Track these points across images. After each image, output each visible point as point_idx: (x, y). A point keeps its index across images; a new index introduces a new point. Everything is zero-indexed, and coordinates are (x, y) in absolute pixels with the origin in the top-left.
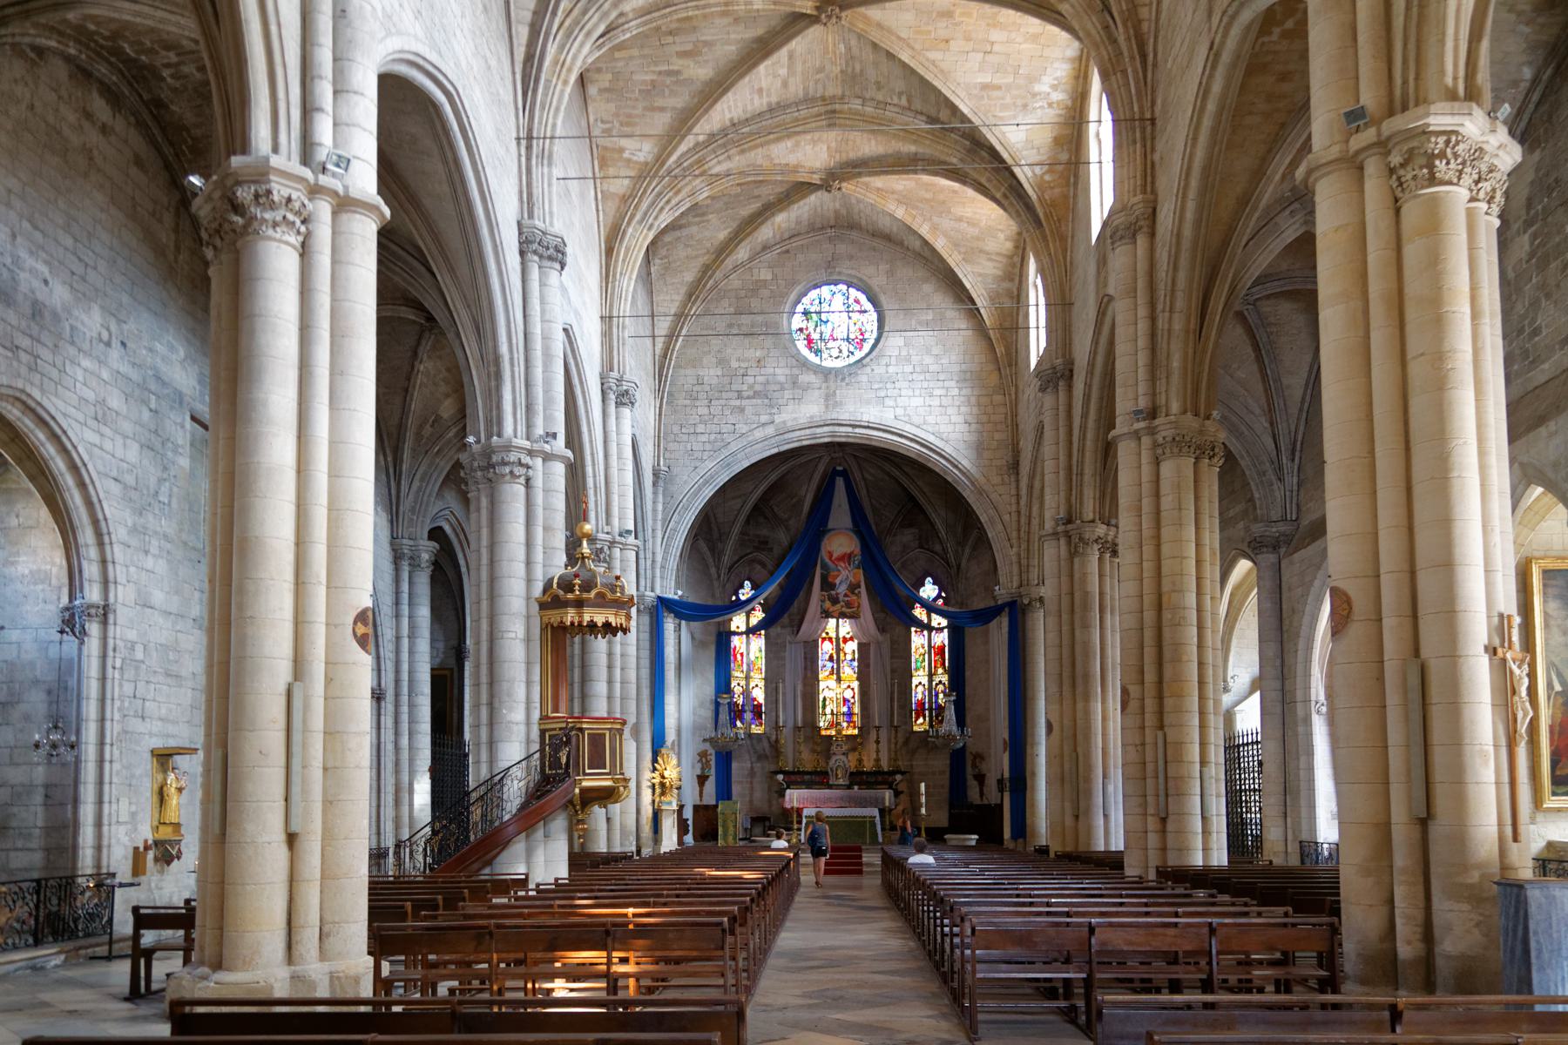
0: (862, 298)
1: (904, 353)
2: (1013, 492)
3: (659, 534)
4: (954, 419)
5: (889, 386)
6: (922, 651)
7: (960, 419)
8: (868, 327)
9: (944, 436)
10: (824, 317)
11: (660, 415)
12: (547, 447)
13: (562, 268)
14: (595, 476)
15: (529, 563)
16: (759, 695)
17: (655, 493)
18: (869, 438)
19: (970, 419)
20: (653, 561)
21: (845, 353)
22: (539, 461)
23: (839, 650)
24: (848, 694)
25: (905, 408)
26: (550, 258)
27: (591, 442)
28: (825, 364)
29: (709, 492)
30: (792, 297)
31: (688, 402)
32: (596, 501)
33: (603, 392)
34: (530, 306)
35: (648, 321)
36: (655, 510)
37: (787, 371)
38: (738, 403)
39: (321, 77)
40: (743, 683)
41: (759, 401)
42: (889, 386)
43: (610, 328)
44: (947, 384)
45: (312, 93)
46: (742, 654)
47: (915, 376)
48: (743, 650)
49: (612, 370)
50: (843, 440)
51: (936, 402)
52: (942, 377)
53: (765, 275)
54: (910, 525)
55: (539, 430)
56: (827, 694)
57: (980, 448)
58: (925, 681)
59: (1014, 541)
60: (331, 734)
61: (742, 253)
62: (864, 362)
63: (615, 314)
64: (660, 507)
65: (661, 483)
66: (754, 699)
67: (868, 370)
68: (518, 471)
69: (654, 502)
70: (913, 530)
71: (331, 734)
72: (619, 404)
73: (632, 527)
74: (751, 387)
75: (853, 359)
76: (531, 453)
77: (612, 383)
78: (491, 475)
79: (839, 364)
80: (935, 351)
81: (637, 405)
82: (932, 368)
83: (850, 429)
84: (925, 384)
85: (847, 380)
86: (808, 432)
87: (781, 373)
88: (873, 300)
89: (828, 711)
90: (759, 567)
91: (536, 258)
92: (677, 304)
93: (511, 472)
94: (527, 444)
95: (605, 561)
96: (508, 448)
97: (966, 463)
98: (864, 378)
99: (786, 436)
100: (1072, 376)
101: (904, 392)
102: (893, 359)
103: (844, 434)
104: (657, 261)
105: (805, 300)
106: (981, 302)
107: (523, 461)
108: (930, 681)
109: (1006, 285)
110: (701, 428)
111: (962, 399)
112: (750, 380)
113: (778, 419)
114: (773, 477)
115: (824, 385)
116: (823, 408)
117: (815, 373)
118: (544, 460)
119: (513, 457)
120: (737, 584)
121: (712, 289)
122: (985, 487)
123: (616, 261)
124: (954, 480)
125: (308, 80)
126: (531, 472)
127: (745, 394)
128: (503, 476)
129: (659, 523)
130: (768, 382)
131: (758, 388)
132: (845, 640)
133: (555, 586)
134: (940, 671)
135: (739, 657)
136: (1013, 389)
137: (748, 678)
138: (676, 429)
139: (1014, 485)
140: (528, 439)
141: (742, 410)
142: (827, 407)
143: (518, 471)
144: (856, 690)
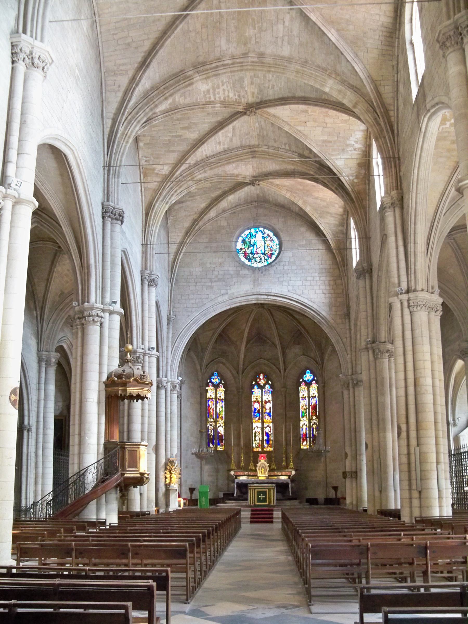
0: (271, 234)
1: (292, 260)
2: (348, 327)
3: (170, 349)
4: (317, 292)
5: (285, 275)
6: (305, 407)
7: (321, 292)
8: (274, 247)
9: (313, 300)
10: (252, 243)
11: (171, 290)
12: (111, 308)
13: (122, 224)
14: (136, 321)
15: (100, 364)
16: (221, 430)
17: (168, 329)
18: (275, 301)
19: (325, 291)
20: (167, 363)
21: (263, 260)
22: (107, 314)
23: (263, 407)
24: (267, 430)
25: (293, 286)
26: (116, 219)
27: (135, 304)
28: (253, 265)
29: (195, 328)
30: (237, 233)
31: (185, 284)
32: (137, 333)
33: (142, 280)
34: (105, 241)
35: (166, 246)
36: (168, 337)
37: (235, 269)
38: (210, 284)
39: (12, 148)
40: (213, 424)
41: (220, 283)
42: (285, 275)
43: (146, 249)
44: (313, 275)
45: (8, 155)
46: (213, 409)
47: (297, 271)
48: (213, 407)
49: (146, 269)
50: (262, 302)
51: (308, 283)
52: (311, 271)
53: (224, 223)
54: (299, 344)
55: (108, 300)
56: (257, 430)
57: (331, 306)
58: (307, 423)
59: (349, 352)
61: (212, 213)
62: (273, 264)
63: (149, 243)
64: (171, 335)
65: (171, 323)
66: (219, 433)
67: (274, 268)
68: (96, 319)
69: (168, 333)
70: (300, 346)
72: (149, 286)
73: (154, 346)
74: (216, 276)
75: (266, 263)
76: (103, 311)
77: (146, 275)
78: (83, 321)
79: (260, 265)
80: (307, 259)
81: (158, 286)
82: (305, 267)
83: (266, 297)
84: (303, 275)
85: (264, 273)
86: (245, 298)
87: (232, 270)
88: (276, 234)
89: (257, 438)
90: (221, 365)
91: (110, 219)
92: (180, 237)
93: (93, 320)
94: (101, 306)
95: (141, 363)
96: (92, 308)
97: (324, 313)
98: (272, 272)
99: (234, 300)
100: (372, 272)
101: (292, 279)
102: (287, 263)
103: (263, 299)
104: (171, 218)
105: (243, 235)
106: (329, 236)
107: (99, 314)
108: (310, 423)
109: (341, 228)
110: (191, 297)
111: (321, 282)
112: (216, 273)
113: (230, 292)
114: (229, 320)
115: (253, 275)
116: (252, 286)
117: (248, 269)
118: (110, 314)
119: (94, 313)
120: (210, 373)
121: (197, 230)
122: (334, 325)
123: (150, 219)
124: (318, 322)
125: (7, 150)
126: (103, 320)
127: (214, 280)
128: (89, 321)
129: (170, 344)
130: (225, 274)
131: (220, 277)
132: (266, 402)
133: (113, 376)
134: (314, 417)
135: (211, 411)
136: (346, 277)
137: (216, 422)
138: (179, 297)
139: (347, 324)
140: (102, 304)
141: (212, 287)
142: (254, 285)
143: (96, 319)
144: (272, 428)
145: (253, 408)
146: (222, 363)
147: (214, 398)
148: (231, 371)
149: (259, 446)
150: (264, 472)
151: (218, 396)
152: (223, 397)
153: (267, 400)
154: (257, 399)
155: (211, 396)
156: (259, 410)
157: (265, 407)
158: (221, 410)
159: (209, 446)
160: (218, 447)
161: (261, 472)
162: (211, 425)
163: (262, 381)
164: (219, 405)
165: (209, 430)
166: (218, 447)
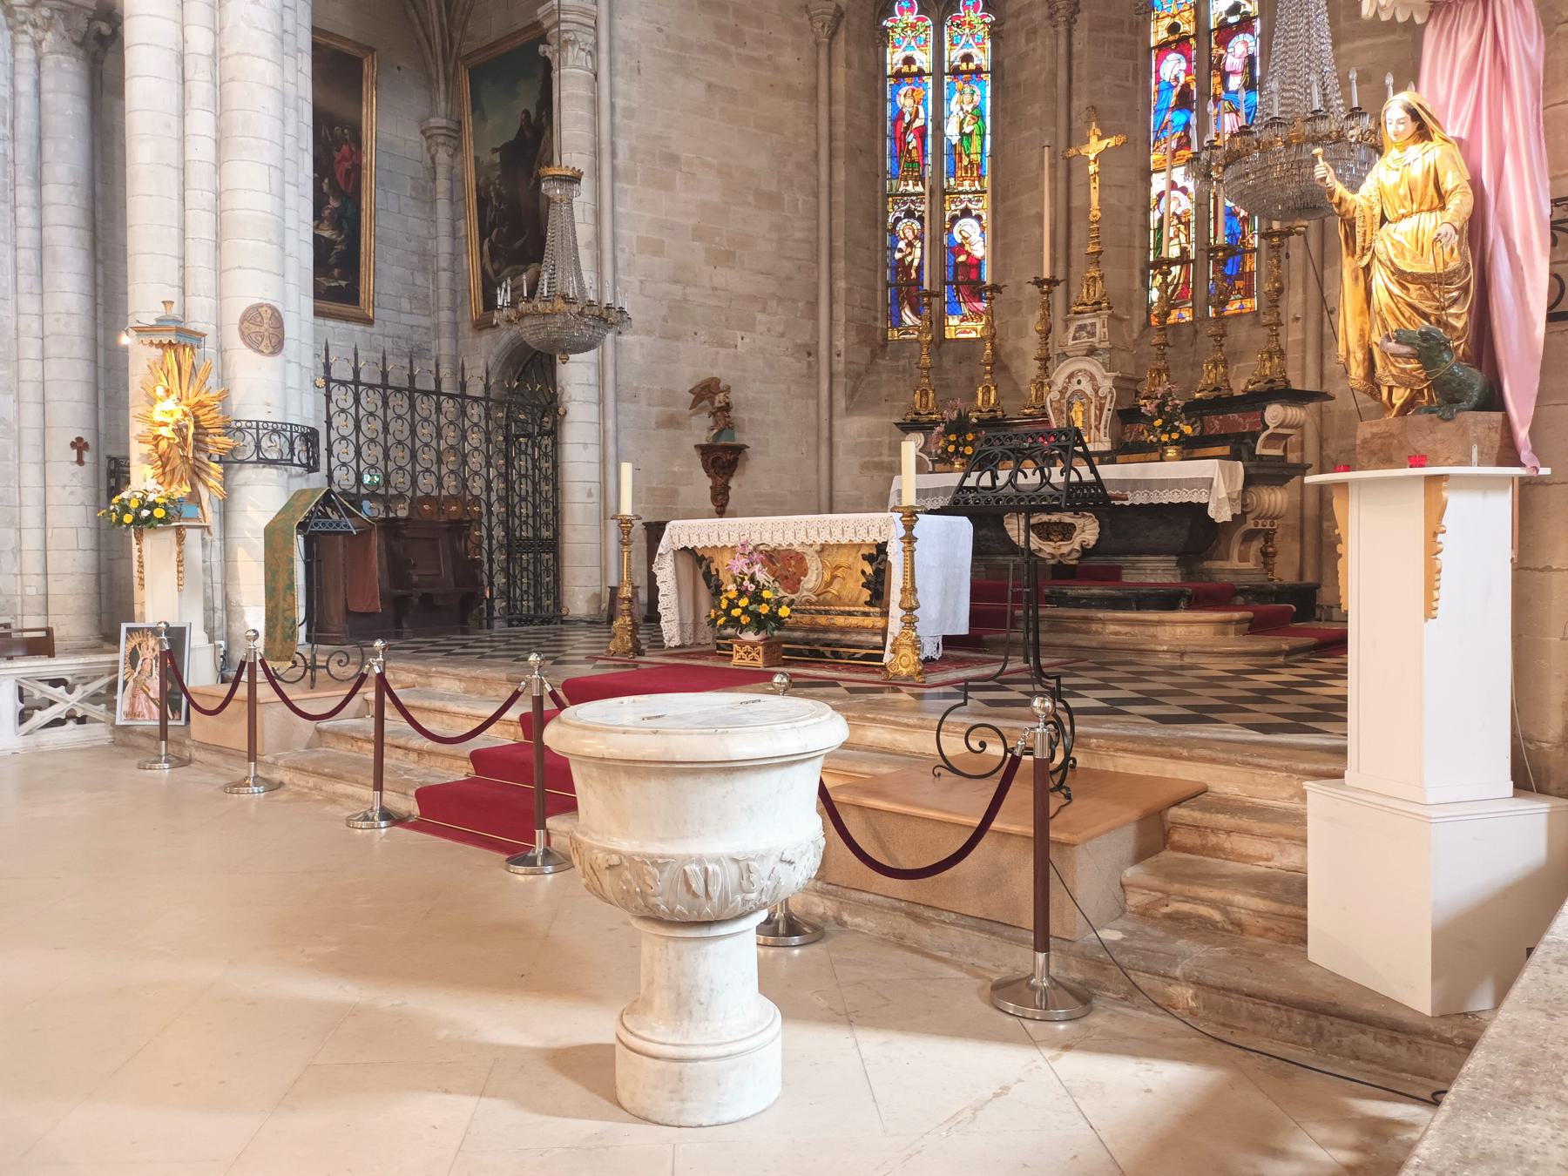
16: (974, 237)
46: (923, 129)
60: (880, 466)
66: (960, 249)
71: (880, 466)
132: (1226, 33)
135: (910, 137)
145: (1154, 88)
147: (927, 67)
149: (1183, 296)
151: (953, 55)
152: (983, 58)
153: (1233, 19)
155: (909, 61)
156: (1187, 85)
158: (967, 130)
159: (898, 322)
160: (953, 321)
162: (909, 214)
164: (955, 109)
165: (896, 240)
166: (953, 321)
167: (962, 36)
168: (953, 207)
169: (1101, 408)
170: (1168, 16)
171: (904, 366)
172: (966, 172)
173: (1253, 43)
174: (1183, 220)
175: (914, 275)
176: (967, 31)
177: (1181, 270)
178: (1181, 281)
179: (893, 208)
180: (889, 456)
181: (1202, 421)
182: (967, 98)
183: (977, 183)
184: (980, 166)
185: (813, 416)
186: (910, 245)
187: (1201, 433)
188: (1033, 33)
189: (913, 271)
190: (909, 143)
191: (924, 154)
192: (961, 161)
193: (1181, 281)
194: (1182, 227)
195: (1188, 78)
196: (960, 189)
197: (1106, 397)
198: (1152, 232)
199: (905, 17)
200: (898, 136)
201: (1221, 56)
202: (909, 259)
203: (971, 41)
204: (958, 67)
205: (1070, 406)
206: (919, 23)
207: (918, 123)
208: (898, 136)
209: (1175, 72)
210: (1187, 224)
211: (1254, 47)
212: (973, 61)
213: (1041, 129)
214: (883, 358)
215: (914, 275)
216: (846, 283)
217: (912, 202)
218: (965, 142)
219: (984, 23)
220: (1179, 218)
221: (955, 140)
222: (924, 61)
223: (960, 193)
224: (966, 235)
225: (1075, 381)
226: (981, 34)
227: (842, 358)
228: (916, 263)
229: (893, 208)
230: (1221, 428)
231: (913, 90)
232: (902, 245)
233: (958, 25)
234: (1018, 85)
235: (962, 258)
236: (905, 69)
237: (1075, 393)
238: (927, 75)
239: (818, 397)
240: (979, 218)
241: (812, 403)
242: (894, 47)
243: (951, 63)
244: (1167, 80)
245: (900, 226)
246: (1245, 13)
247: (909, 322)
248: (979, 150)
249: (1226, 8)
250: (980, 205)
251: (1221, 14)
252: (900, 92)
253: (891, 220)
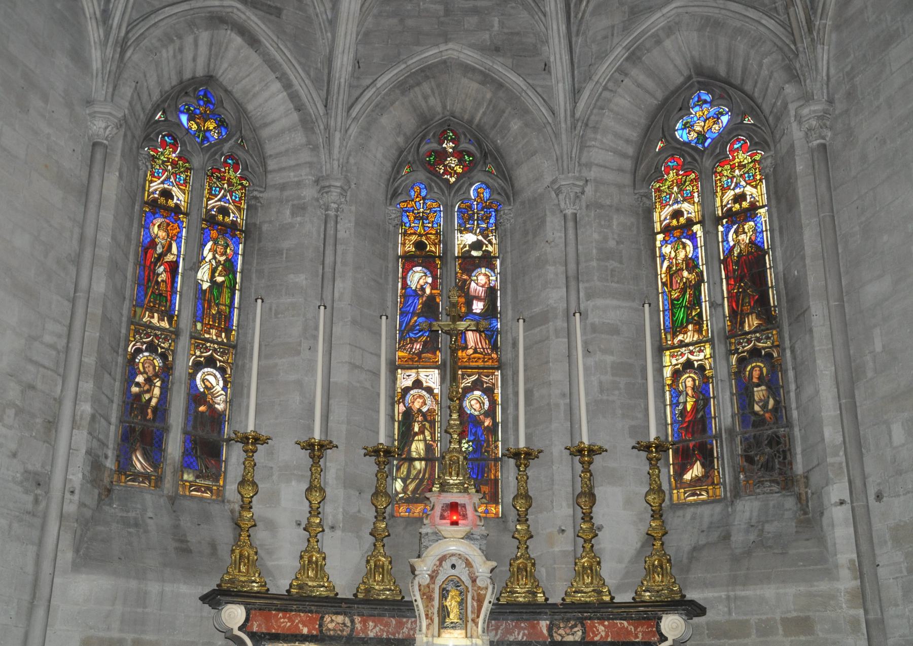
46: (173, 268)
89: (417, 447)
90: (238, 40)
132: (469, 263)
146: (243, 31)
148: (287, 85)
150: (463, 617)
154: (420, 245)
156: (432, 298)
157: (463, 288)
158: (220, 279)
161: (444, 612)
162: (152, 348)
163: (452, 162)
165: (134, 373)
167: (221, 189)
168: (198, 353)
169: (480, 601)
170: (415, 234)
171: (135, 519)
172: (214, 321)
173: (494, 278)
174: (429, 419)
175: (150, 415)
176: (226, 186)
177: (426, 465)
178: (427, 476)
179: (134, 337)
180: (121, 631)
181: (583, 625)
182: (220, 249)
183: (223, 335)
184: (229, 318)
185: (30, 568)
186: (149, 381)
187: (583, 638)
188: (299, 209)
189: (149, 411)
190: (158, 275)
191: (173, 291)
192: (210, 307)
193: (427, 476)
194: (427, 425)
195: (434, 291)
196: (207, 336)
197: (487, 588)
198: (396, 424)
199: (167, 152)
200: (148, 263)
201: (465, 280)
202: (147, 396)
203: (228, 197)
204: (214, 216)
205: (444, 594)
206: (181, 163)
207: (170, 258)
208: (148, 263)
209: (422, 282)
210: (432, 423)
211: (495, 280)
212: (229, 216)
213: (305, 300)
214: (110, 505)
215: (150, 415)
216: (92, 407)
217: (156, 336)
218: (215, 292)
219: (241, 184)
220: (424, 415)
221: (205, 286)
222: (181, 198)
223: (207, 340)
224: (209, 385)
225: (447, 565)
226: (238, 194)
227: (76, 497)
228: (154, 402)
229: (134, 337)
230: (607, 636)
231: (168, 225)
232: (140, 379)
233: (218, 178)
234: (279, 252)
235: (202, 408)
236: (162, 200)
237: (448, 580)
238: (183, 214)
239: (40, 544)
240: (222, 371)
241: (32, 550)
242: (153, 175)
243: (208, 211)
244: (414, 288)
245: (141, 358)
246: (486, 251)
247: (139, 466)
248: (228, 301)
249: (470, 243)
250: (225, 358)
251: (465, 246)
252: (155, 221)
253: (130, 349)
